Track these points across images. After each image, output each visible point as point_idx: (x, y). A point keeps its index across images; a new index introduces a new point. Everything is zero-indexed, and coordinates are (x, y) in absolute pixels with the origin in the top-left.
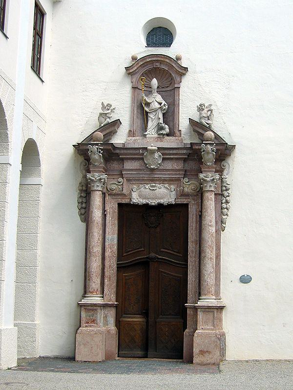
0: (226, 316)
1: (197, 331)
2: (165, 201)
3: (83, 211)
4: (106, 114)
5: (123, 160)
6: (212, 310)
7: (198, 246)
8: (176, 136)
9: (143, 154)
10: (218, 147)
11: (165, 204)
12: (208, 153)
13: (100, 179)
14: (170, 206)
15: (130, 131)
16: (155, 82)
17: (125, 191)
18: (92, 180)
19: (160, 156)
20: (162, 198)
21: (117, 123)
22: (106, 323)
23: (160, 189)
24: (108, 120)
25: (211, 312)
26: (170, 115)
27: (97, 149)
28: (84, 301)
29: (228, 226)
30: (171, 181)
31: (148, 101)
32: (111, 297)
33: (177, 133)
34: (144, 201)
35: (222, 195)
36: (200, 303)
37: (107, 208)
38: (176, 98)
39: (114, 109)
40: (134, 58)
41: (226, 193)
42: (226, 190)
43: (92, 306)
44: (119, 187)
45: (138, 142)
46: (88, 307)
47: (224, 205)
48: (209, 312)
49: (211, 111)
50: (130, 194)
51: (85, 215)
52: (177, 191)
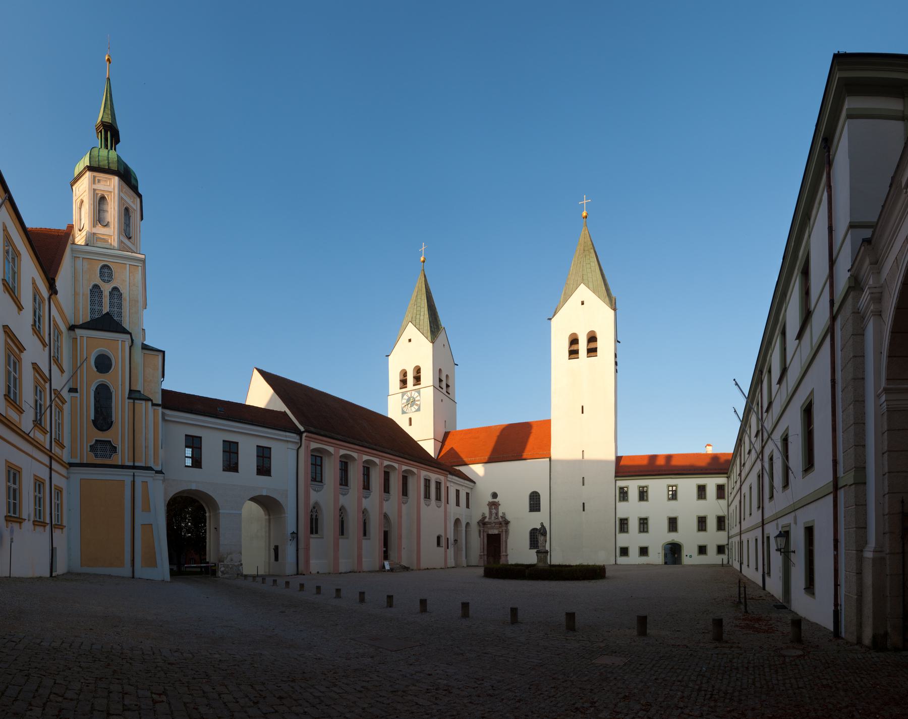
0: (508, 557)
16: (493, 507)
26: (497, 514)
32: (486, 553)
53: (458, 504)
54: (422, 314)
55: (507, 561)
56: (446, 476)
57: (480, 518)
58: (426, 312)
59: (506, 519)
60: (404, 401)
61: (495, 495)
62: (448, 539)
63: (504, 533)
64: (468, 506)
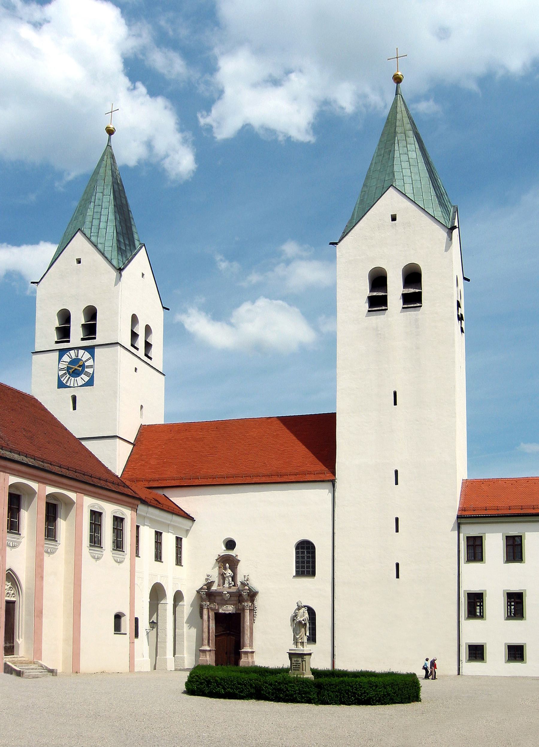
1: (242, 660)
8: (236, 587)
16: (227, 565)
21: (212, 582)
24: (209, 581)
26: (234, 578)
31: (225, 572)
33: (237, 586)
35: (254, 610)
36: (242, 650)
40: (219, 555)
45: (220, 589)
47: (255, 614)
53: (158, 557)
54: (103, 219)
55: (253, 662)
56: (134, 508)
57: (200, 583)
58: (111, 217)
59: (250, 589)
60: (63, 365)
61: (230, 544)
62: (137, 620)
63: (247, 613)
64: (179, 562)
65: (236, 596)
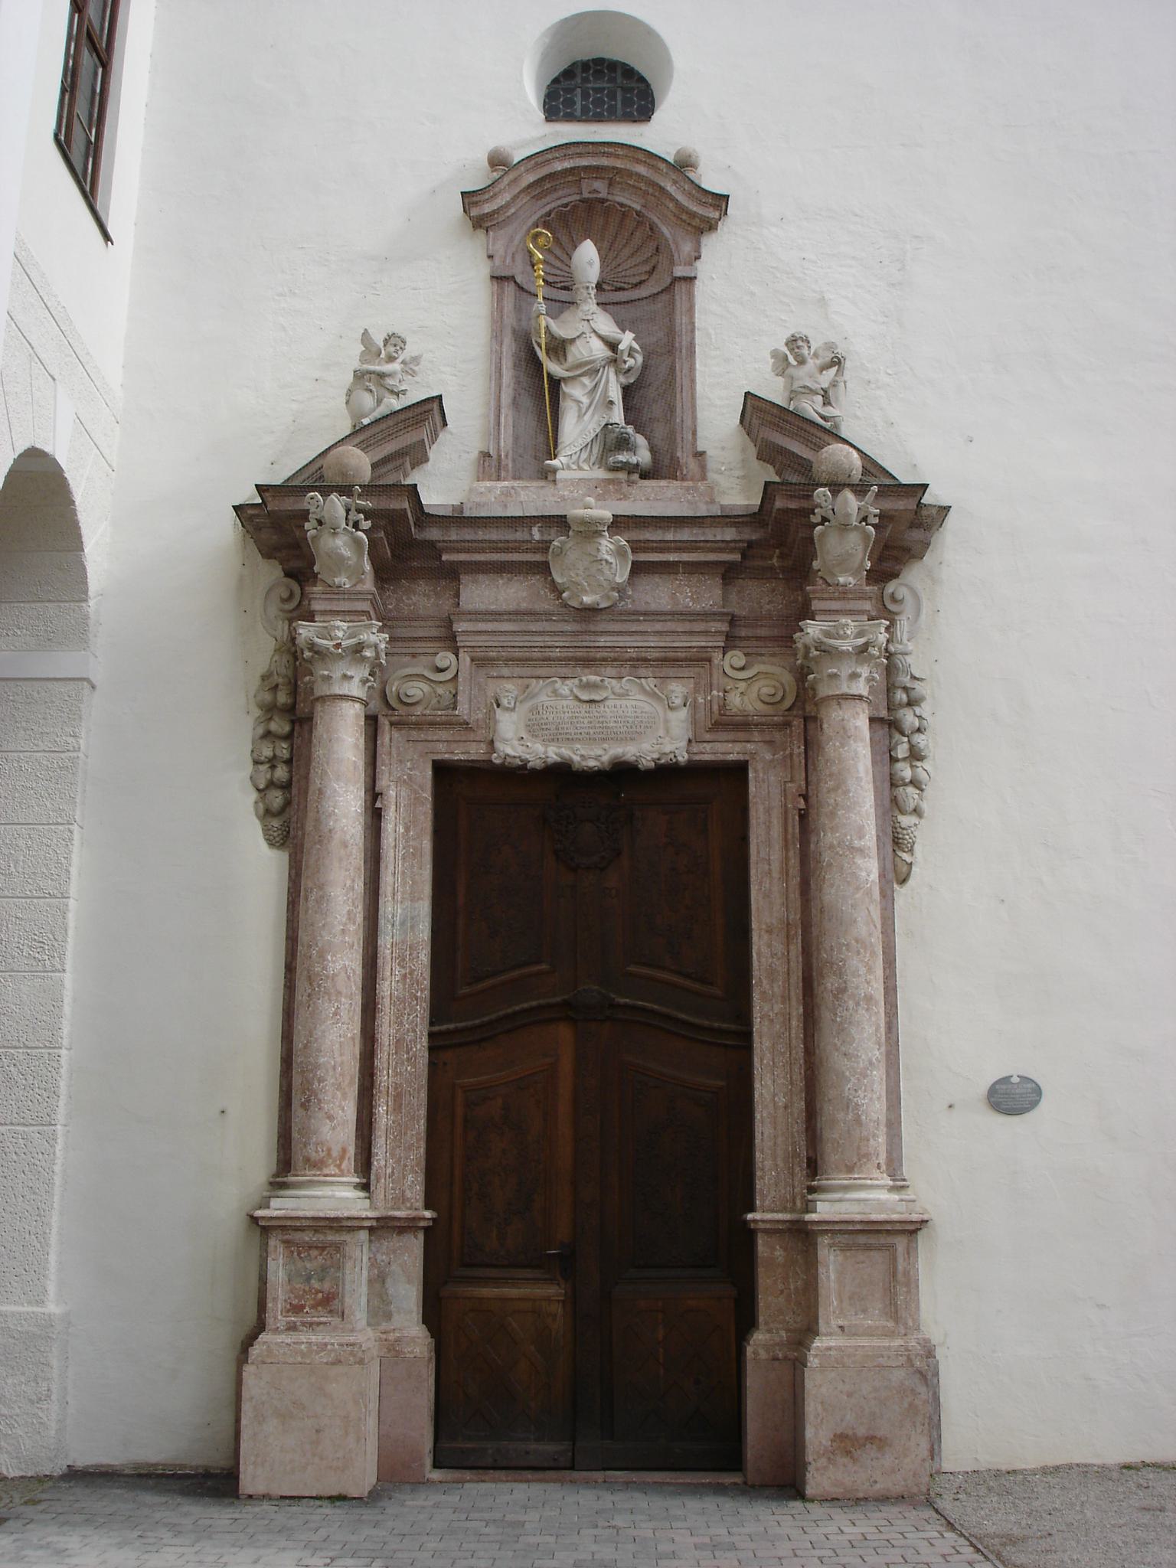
1: (818, 1343)
2: (645, 751)
3: (276, 798)
4: (382, 376)
5: (452, 574)
6: (883, 1240)
7: (796, 949)
9: (544, 546)
10: (889, 504)
11: (647, 763)
12: (845, 527)
13: (359, 648)
14: (667, 773)
15: (486, 455)
16: (588, 257)
17: (463, 710)
18: (319, 653)
19: (620, 552)
20: (631, 738)
22: (381, 1310)
23: (621, 696)
25: (879, 1248)
27: (348, 511)
28: (281, 1207)
29: (923, 858)
30: (668, 662)
31: (561, 331)
33: (691, 465)
34: (553, 753)
36: (825, 1209)
37: (383, 783)
38: (681, 320)
39: (416, 360)
40: (497, 161)
41: (908, 718)
42: (911, 703)
43: (316, 1230)
44: (440, 690)
46: (297, 1236)
48: (868, 1248)
49: (837, 362)
50: (490, 721)
51: (286, 816)
52: (695, 706)
65: (693, 568)
